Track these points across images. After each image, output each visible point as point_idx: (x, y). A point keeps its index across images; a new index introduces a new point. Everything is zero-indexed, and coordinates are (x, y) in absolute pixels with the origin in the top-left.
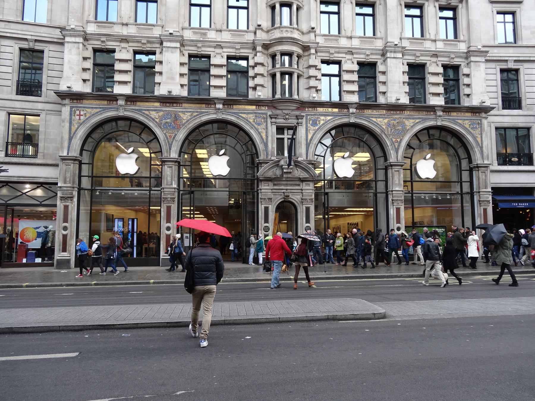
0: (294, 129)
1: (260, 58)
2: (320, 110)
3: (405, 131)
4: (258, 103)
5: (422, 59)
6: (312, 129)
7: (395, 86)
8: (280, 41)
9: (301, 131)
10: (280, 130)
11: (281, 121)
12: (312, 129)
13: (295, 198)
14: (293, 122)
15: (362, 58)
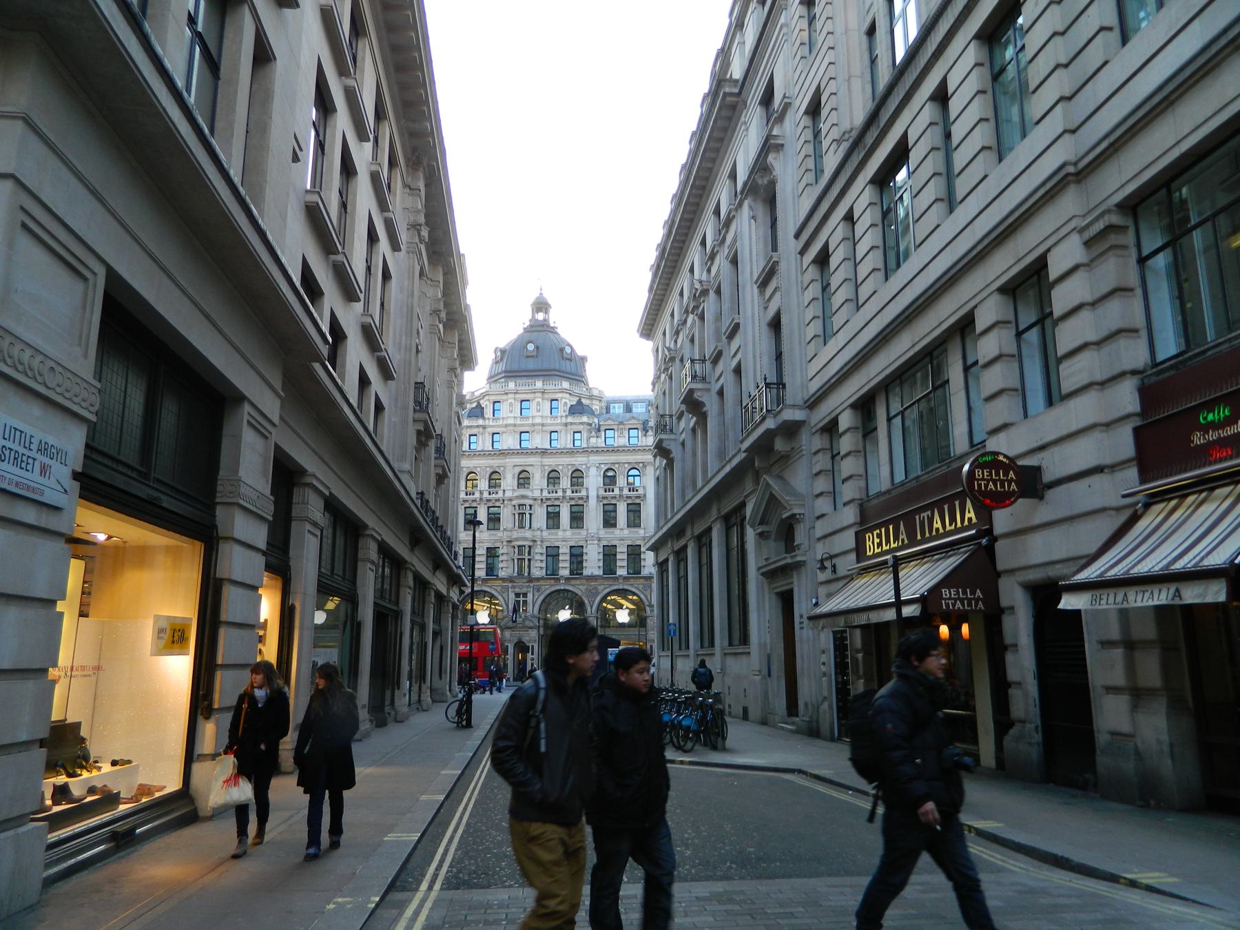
0: (525, 595)
1: (504, 551)
2: (542, 582)
3: (597, 594)
4: (503, 580)
5: (614, 543)
6: (537, 594)
7: (593, 564)
8: (517, 539)
9: (530, 596)
10: (517, 595)
11: (517, 590)
12: (537, 594)
13: (525, 639)
14: (524, 590)
15: (572, 544)
